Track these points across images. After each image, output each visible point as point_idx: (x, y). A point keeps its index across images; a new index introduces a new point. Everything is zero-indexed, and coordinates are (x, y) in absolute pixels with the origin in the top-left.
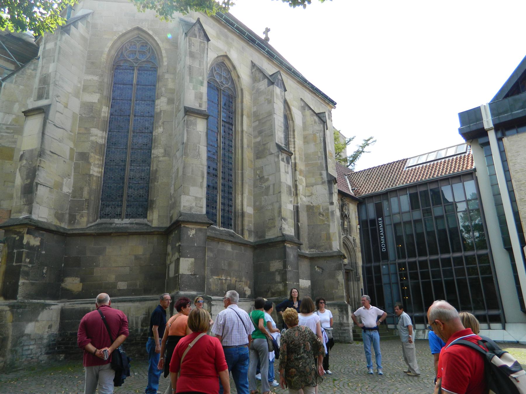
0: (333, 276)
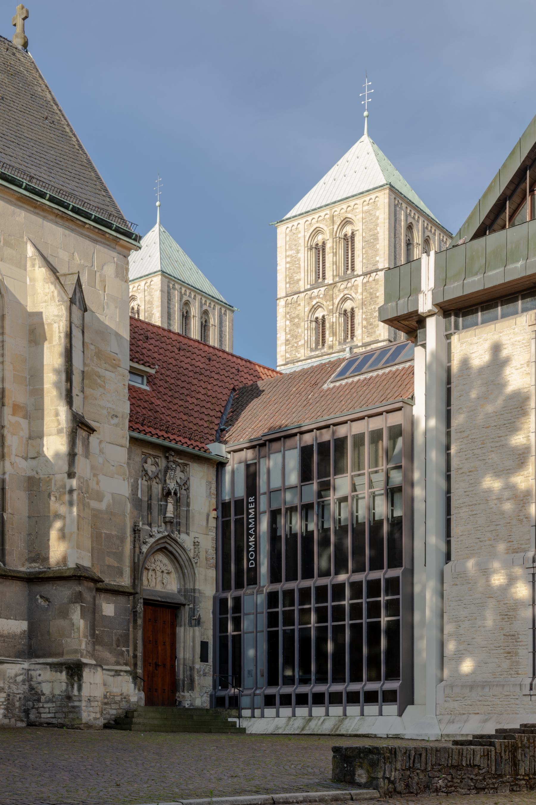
0: (64, 614)
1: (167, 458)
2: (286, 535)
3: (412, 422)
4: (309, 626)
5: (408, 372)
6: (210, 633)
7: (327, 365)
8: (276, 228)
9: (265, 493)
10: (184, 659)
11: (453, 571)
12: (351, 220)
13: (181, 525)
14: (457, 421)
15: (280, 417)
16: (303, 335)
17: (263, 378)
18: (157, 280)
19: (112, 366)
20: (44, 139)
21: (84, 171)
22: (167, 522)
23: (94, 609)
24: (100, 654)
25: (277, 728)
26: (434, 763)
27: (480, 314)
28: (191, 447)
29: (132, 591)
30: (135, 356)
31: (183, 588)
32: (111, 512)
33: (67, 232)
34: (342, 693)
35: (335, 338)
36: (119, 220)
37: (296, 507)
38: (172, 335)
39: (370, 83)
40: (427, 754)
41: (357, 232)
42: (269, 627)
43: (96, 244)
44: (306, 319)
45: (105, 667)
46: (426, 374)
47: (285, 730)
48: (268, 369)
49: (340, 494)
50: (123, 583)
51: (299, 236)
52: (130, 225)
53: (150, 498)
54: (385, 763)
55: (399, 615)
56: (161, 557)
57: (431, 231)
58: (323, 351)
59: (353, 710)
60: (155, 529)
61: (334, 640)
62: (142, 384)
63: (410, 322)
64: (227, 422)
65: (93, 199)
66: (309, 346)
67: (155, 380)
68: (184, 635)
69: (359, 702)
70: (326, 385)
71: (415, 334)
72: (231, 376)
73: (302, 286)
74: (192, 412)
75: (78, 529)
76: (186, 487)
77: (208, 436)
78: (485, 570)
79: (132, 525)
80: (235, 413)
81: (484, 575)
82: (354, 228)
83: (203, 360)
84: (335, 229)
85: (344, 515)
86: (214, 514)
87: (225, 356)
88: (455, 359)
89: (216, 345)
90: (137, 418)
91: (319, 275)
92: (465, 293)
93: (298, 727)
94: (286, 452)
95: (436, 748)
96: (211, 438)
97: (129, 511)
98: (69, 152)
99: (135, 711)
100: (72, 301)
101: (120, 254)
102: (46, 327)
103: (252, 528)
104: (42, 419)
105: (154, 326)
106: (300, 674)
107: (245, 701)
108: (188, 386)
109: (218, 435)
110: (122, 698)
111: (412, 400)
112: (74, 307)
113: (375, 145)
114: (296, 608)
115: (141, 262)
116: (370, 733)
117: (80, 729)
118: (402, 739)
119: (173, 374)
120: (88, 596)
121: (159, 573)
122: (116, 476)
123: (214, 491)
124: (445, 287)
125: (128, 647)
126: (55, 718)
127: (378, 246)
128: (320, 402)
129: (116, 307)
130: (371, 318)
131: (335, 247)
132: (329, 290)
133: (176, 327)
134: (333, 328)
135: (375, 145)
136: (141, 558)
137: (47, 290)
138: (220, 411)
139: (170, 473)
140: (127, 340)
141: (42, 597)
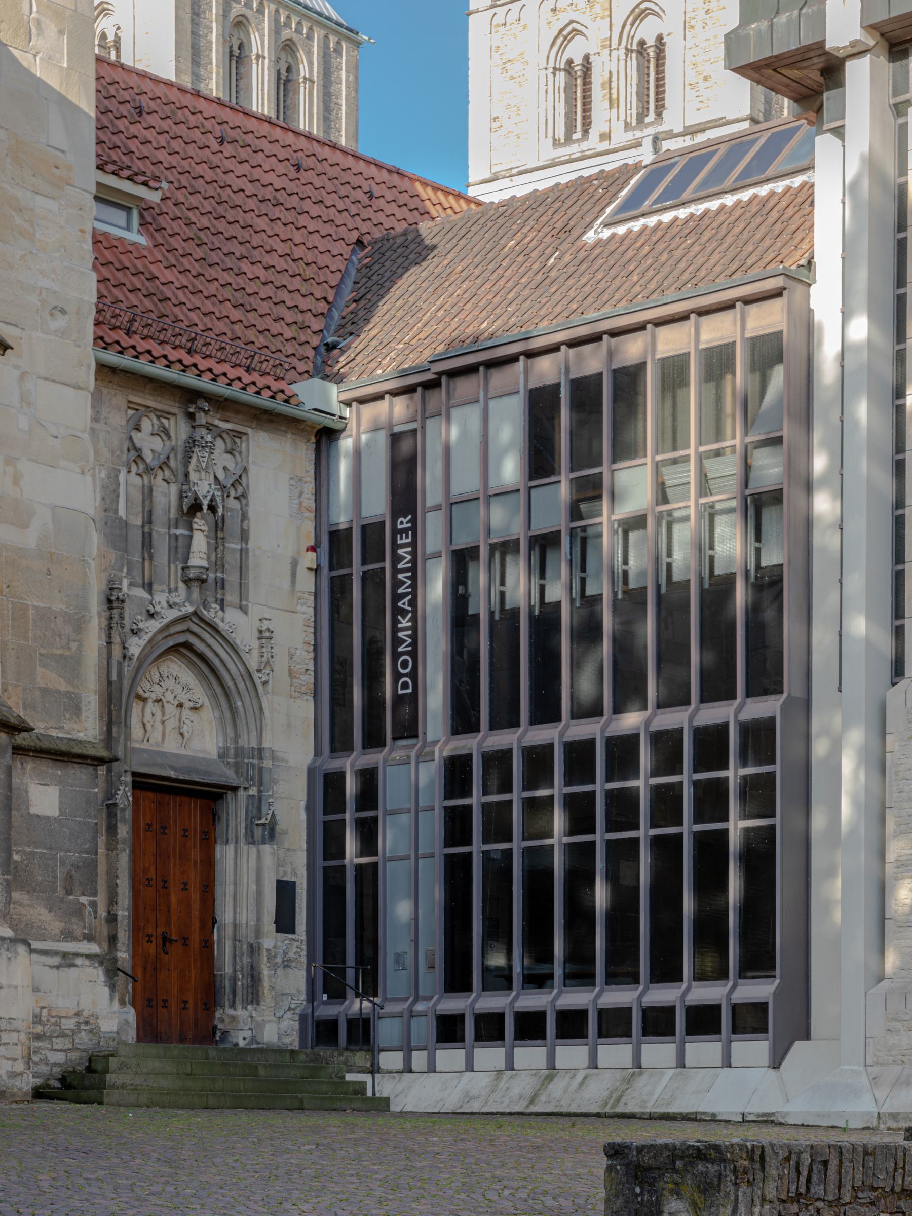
1: (191, 416)
2: (492, 614)
4: (548, 841)
6: (300, 860)
7: (595, 182)
9: (438, 508)
10: (235, 926)
13: (227, 586)
15: (475, 313)
17: (434, 213)
22: (190, 580)
23: (9, 799)
24: (24, 912)
25: (468, 1097)
26: (858, 1183)
28: (252, 389)
29: (103, 753)
30: (109, 156)
31: (232, 746)
32: (51, 554)
34: (630, 1009)
35: (614, 111)
37: (517, 542)
38: (202, 105)
40: (841, 1162)
42: (446, 845)
45: (35, 945)
46: (844, 203)
47: (487, 1102)
48: (447, 192)
49: (627, 509)
53: (149, 519)
54: (736, 1184)
55: (773, 816)
56: (175, 667)
60: (161, 598)
61: (612, 878)
62: (128, 228)
63: (805, 72)
66: (550, 134)
67: (160, 218)
69: (674, 1034)
71: (817, 104)
72: (354, 209)
74: (254, 302)
76: (240, 490)
77: (294, 361)
79: (104, 587)
80: (362, 303)
83: (281, 168)
86: (310, 559)
87: (338, 157)
90: (115, 316)
94: (492, 403)
95: (865, 1146)
96: (302, 367)
97: (95, 552)
99: (112, 1055)
103: (404, 595)
105: (156, 80)
106: (527, 962)
108: (245, 235)
109: (319, 360)
110: (78, 1024)
111: (810, 270)
114: (517, 796)
116: (700, 1110)
118: (781, 1124)
119: (205, 203)
121: (170, 709)
125: (95, 895)
128: (576, 275)
129: (61, 32)
133: (214, 86)
134: (610, 89)
136: (127, 670)
138: (325, 299)
140: (89, 116)
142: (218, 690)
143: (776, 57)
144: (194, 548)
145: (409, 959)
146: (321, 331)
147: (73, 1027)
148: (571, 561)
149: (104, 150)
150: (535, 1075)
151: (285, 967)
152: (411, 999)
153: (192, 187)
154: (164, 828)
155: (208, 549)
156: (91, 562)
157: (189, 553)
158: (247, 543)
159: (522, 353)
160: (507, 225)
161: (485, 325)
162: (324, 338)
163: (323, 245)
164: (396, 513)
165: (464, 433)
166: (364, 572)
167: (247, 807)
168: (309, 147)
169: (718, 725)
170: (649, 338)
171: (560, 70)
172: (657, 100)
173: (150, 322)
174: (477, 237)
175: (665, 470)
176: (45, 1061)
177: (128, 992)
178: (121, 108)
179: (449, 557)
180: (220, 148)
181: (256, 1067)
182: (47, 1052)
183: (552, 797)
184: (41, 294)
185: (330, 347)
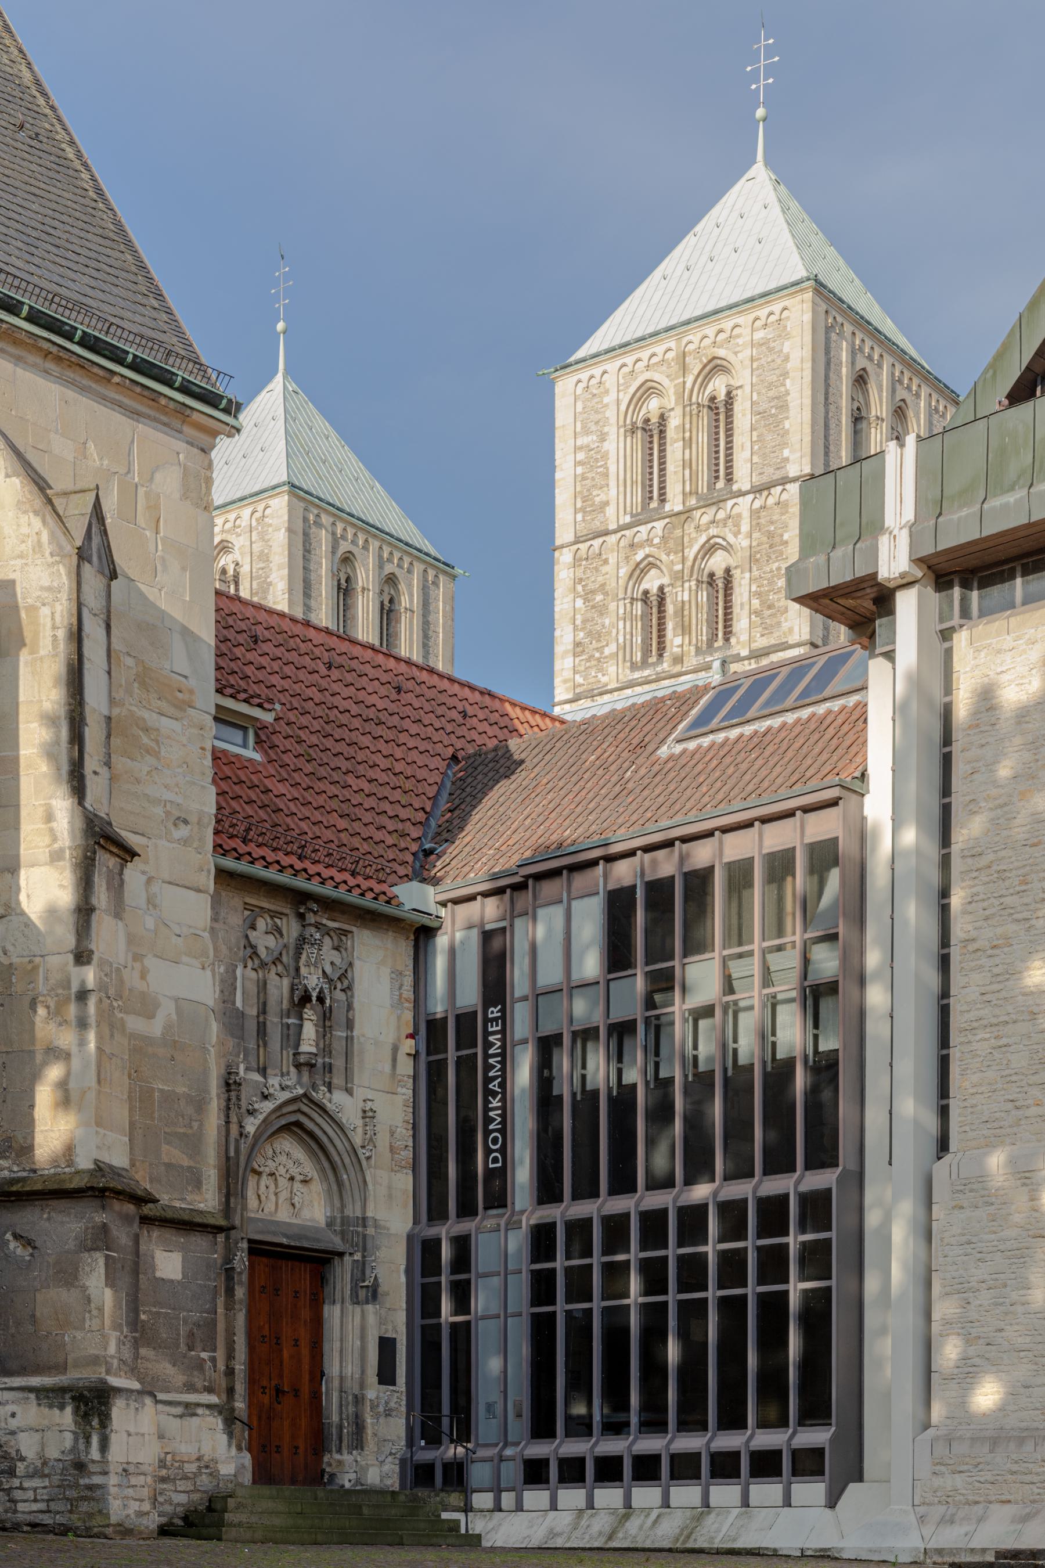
1: (301, 917)
3: (862, 835)
4: (625, 1302)
5: (854, 717)
6: (401, 1318)
7: (668, 702)
8: (552, 384)
9: (525, 998)
10: (342, 1378)
11: (954, 1176)
12: (724, 363)
13: (334, 1070)
14: (965, 831)
15: (559, 821)
16: (614, 631)
17: (522, 731)
18: (280, 505)
19: (176, 706)
20: (15, 175)
21: (108, 251)
23: (137, 1264)
24: (150, 1366)
25: (553, 1534)
27: (1019, 581)
29: (222, 1222)
30: (228, 681)
31: (339, 1215)
32: (175, 1042)
33: (71, 394)
34: (699, 1454)
36: (191, 365)
38: (312, 634)
39: (771, 41)
41: (739, 392)
42: (533, 1304)
43: (138, 421)
44: (621, 596)
45: (161, 1396)
46: (894, 720)
47: (569, 1538)
48: (534, 712)
49: (697, 1000)
50: (202, 1205)
51: (606, 400)
52: (214, 377)
53: (263, 1010)
55: (830, 1278)
56: (287, 1144)
57: (909, 388)
58: (659, 669)
59: (725, 1493)
60: (274, 1081)
61: (683, 1335)
62: (245, 746)
63: (859, 601)
64: (439, 834)
65: (128, 315)
66: (628, 658)
67: (274, 737)
68: (342, 1325)
70: (665, 747)
71: (870, 630)
72: (449, 728)
73: (612, 517)
74: (359, 812)
75: (99, 1082)
76: (346, 983)
77: (395, 866)
78: (1027, 1175)
79: (223, 1071)
80: (457, 813)
81: (1024, 1185)
82: (732, 382)
83: (383, 691)
84: (689, 385)
85: (706, 1049)
86: (409, 1045)
88: (961, 686)
89: (416, 657)
90: (233, 826)
91: (651, 492)
92: (984, 534)
93: (600, 1533)
94: (574, 903)
96: (402, 871)
97: (214, 1039)
98: (75, 206)
99: (230, 1496)
100: (82, 555)
101: (192, 444)
102: (23, 615)
103: (495, 1078)
104: (17, 829)
105: (271, 612)
106: (606, 1411)
107: (479, 1473)
109: (418, 864)
110: (200, 1468)
112: (87, 569)
113: (782, 188)
114: (597, 1260)
115: (242, 464)
116: (763, 1546)
117: (106, 1538)
118: (837, 1559)
119: (314, 722)
120: (122, 1235)
121: (283, 1182)
122: (185, 959)
123: (408, 993)
124: (940, 519)
125: (214, 1351)
126: (49, 1511)
127: (787, 424)
129: (184, 569)
130: (769, 591)
131: (687, 426)
132: (674, 528)
133: (324, 616)
134: (683, 617)
135: (782, 186)
136: (244, 1147)
137: (25, 530)
138: (423, 809)
139: (309, 953)
140: (209, 645)
141: (17, 1237)
142: (326, 1164)
143: (833, 587)
144: (304, 1036)
145: (499, 1409)
146: (420, 838)
147: (194, 1470)
148: (646, 1046)
149: (223, 675)
150: (613, 1514)
151: (386, 1415)
152: (501, 1444)
153: (303, 708)
154: (277, 1290)
155: (317, 1037)
156: (212, 1049)
157: (299, 1040)
158: (352, 1031)
159: (601, 858)
160: (588, 741)
161: (568, 832)
162: (422, 845)
163: (421, 760)
164: (487, 1003)
165: (549, 931)
166: (458, 1057)
167: (352, 1271)
168: (409, 671)
169: (780, 1195)
170: (717, 844)
171: (637, 599)
172: (725, 627)
173: (264, 830)
174: (561, 753)
175: (732, 964)
176: (169, 1501)
177: (244, 1438)
178: (238, 636)
179: (536, 1043)
180: (327, 673)
181: (360, 1507)
182: (171, 1493)
183: (629, 1261)
184: (165, 806)
185: (428, 853)
